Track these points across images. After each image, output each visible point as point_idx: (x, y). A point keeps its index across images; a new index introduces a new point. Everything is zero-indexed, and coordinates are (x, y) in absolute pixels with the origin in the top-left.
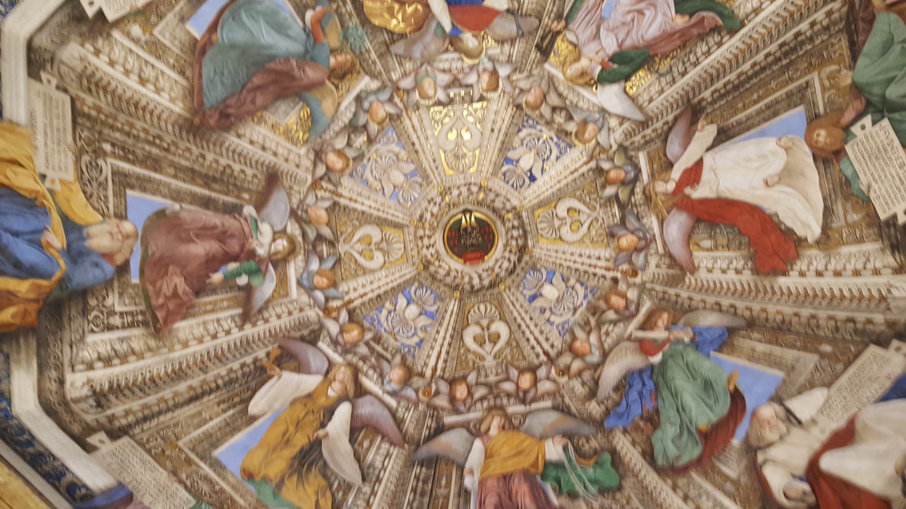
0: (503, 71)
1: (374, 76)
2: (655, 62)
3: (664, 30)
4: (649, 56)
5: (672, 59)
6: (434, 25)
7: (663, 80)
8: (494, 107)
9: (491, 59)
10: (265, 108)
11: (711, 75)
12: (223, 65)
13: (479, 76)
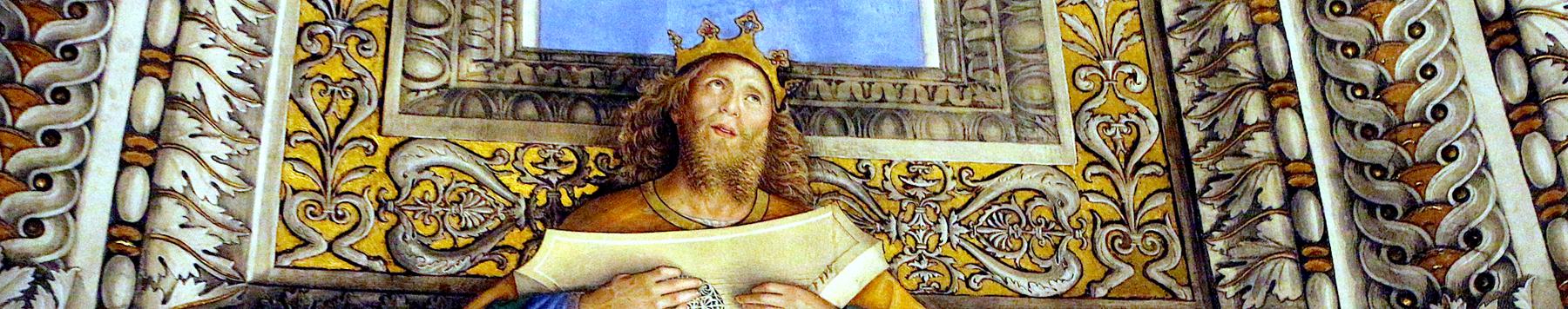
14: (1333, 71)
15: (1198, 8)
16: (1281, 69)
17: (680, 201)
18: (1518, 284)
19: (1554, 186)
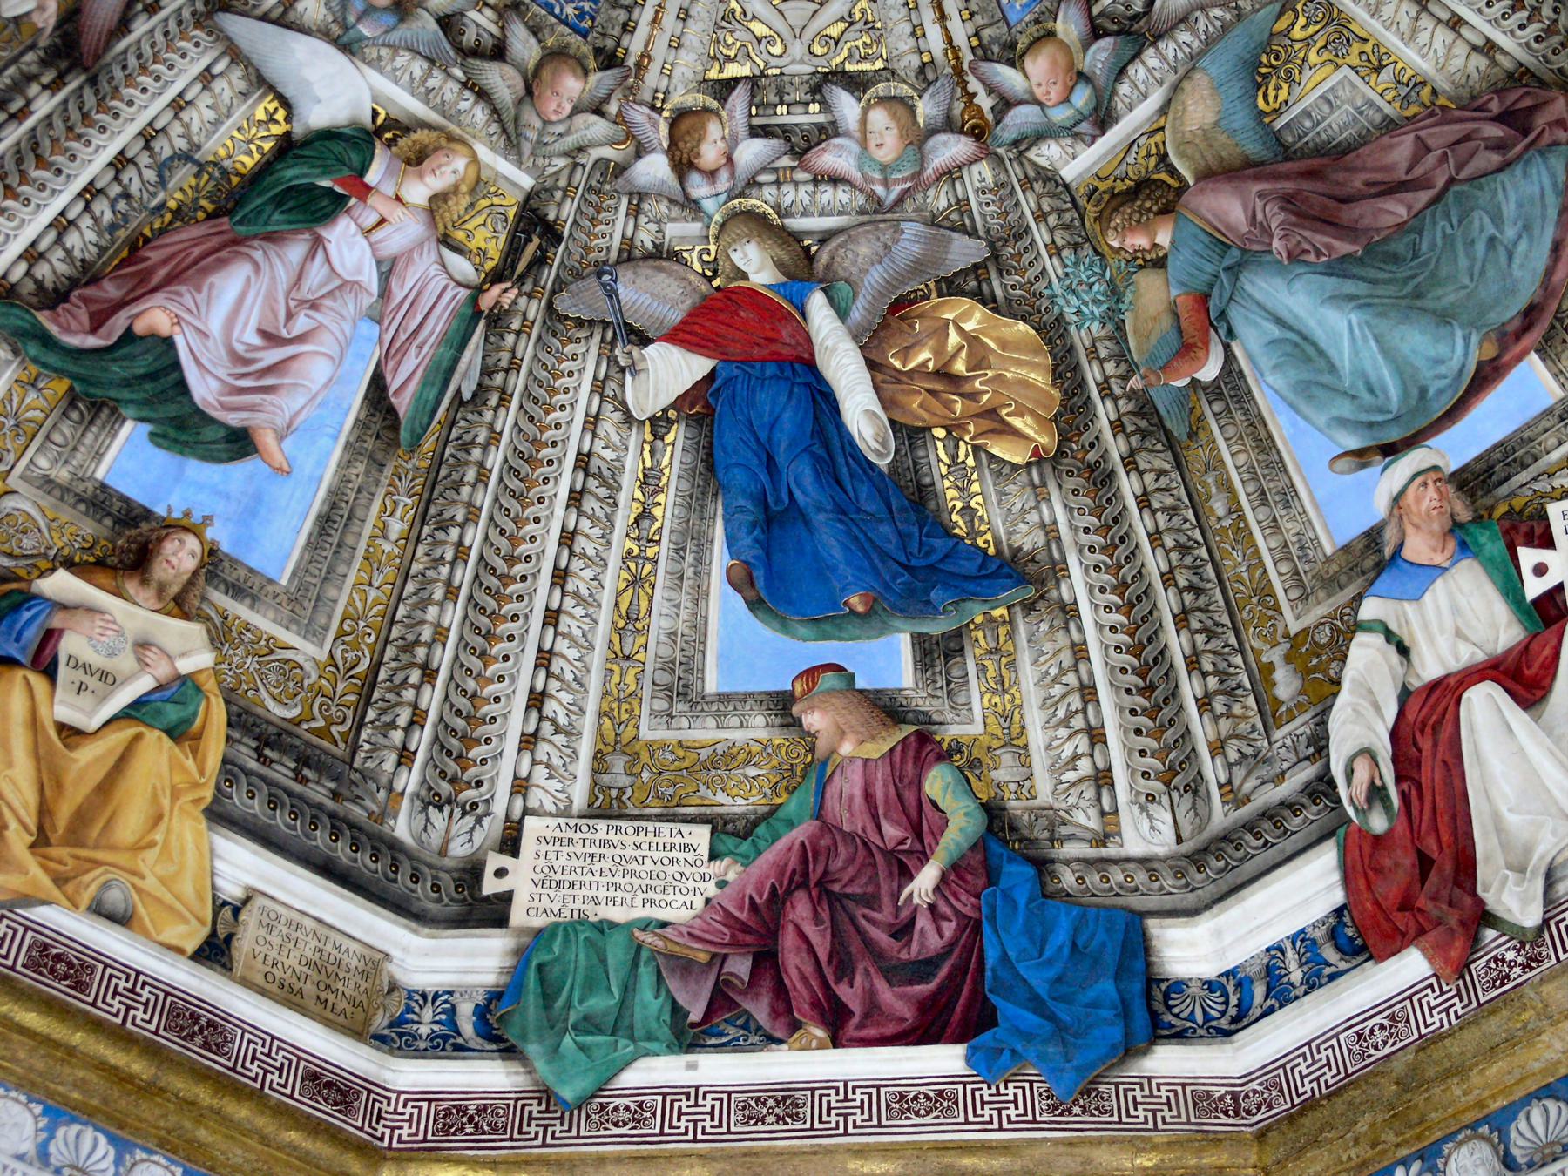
0: (654, 169)
1: (1048, 178)
2: (209, 198)
3: (199, 290)
4: (230, 213)
5: (162, 205)
6: (857, 313)
7: (181, 144)
8: (687, 64)
9: (691, 206)
10: (1390, 126)
11: (41, 162)
12: (1483, 272)
13: (730, 160)
14: (457, 677)
16: (435, 666)
17: (131, 586)
18: (488, 814)
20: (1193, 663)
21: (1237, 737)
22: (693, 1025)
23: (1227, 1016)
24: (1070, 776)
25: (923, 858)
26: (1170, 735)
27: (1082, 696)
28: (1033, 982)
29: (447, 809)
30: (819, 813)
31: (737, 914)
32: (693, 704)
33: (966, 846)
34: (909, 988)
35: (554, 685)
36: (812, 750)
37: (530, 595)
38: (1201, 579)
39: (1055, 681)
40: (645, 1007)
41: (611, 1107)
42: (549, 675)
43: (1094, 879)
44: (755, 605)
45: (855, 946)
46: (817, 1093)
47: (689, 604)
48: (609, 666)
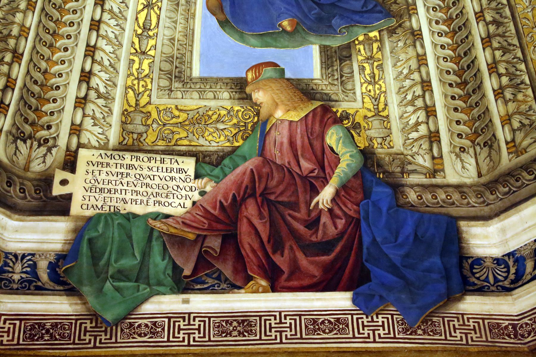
15: (7, 20)
16: (21, 51)
18: (55, 146)
19: (78, 125)
20: (493, 68)
21: (520, 113)
22: (186, 277)
23: (508, 280)
24: (414, 135)
25: (325, 181)
26: (475, 112)
27: (423, 87)
28: (391, 256)
29: (29, 142)
30: (262, 152)
31: (212, 211)
32: (184, 83)
33: (351, 174)
34: (317, 258)
35: (97, 68)
36: (258, 114)
37: (81, 10)
38: (501, 16)
39: (406, 77)
40: (156, 266)
41: (136, 324)
42: (94, 61)
43: (428, 197)
44: (223, 24)
45: (284, 232)
46: (263, 318)
47: (182, 21)
48: (132, 57)
